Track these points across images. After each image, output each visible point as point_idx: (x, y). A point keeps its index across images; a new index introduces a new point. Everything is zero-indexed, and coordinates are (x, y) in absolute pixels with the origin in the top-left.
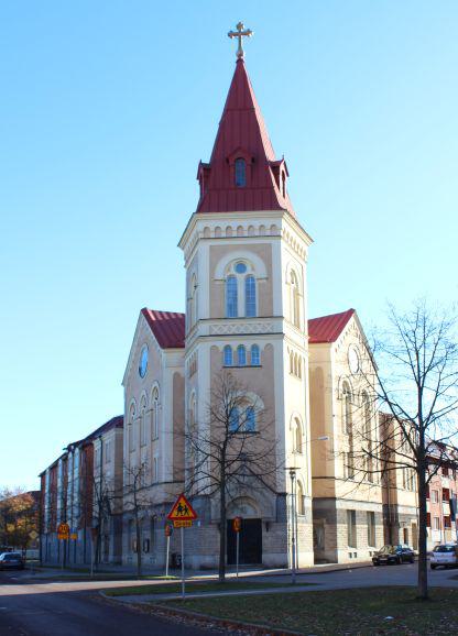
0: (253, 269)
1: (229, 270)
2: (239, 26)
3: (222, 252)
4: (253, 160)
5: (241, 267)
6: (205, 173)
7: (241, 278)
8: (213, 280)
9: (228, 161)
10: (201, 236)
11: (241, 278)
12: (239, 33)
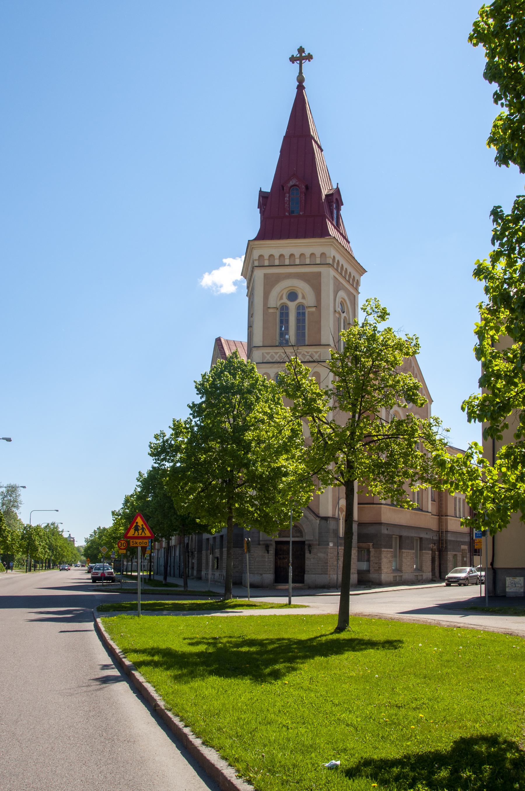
0: (304, 298)
1: (281, 298)
2: (301, 50)
3: (278, 278)
4: (307, 188)
5: (293, 296)
6: (264, 199)
7: (292, 306)
8: (266, 307)
9: (283, 187)
10: (256, 264)
11: (292, 306)
12: (301, 57)
